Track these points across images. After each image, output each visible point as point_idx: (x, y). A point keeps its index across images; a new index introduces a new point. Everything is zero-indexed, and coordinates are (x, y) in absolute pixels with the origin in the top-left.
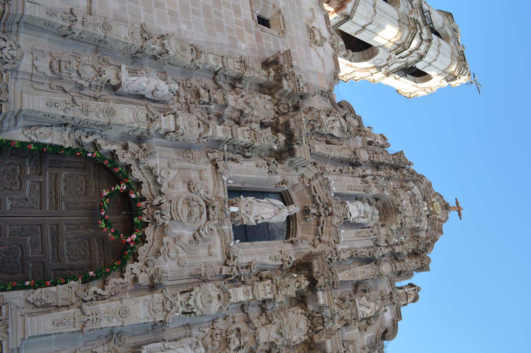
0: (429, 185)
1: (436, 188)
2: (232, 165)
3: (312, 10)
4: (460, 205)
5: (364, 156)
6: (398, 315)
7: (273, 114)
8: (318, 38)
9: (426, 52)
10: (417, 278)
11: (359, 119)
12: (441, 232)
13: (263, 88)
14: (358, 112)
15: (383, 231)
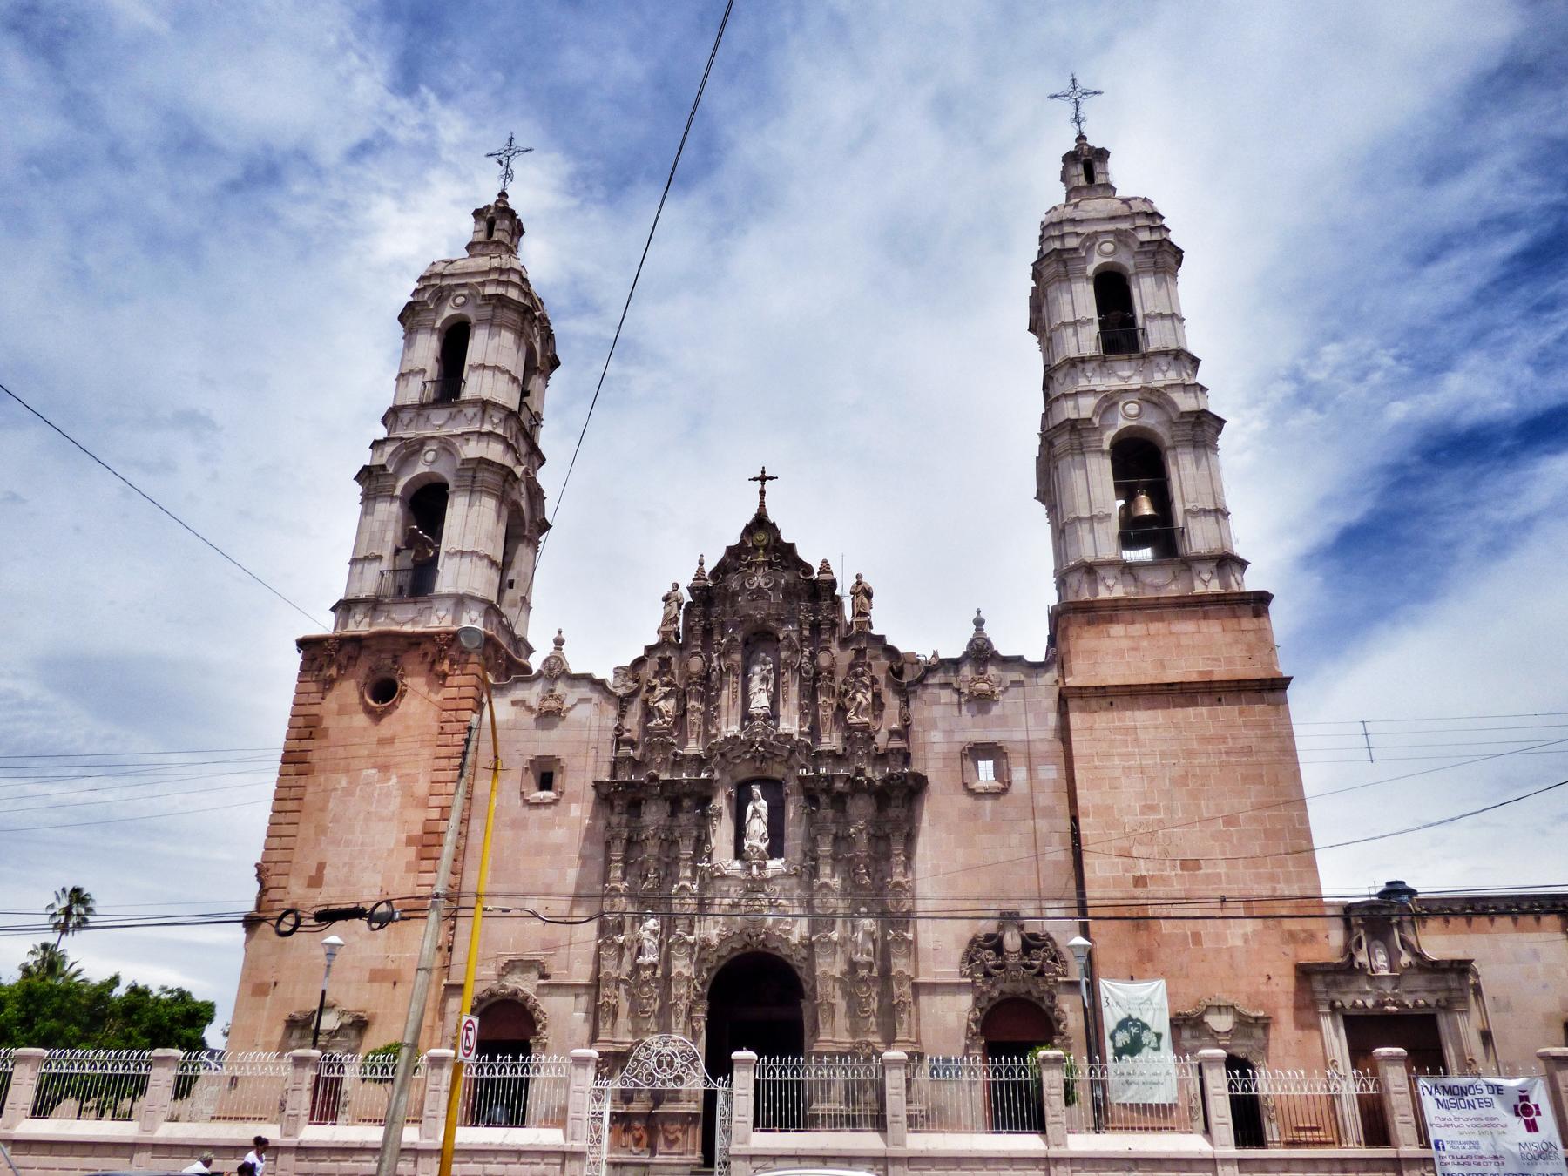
0: (729, 549)
1: (735, 540)
2: (716, 859)
3: (514, 703)
4: (759, 475)
5: (696, 664)
6: (881, 638)
7: (660, 802)
8: (553, 704)
9: (504, 407)
10: (844, 589)
11: (650, 650)
12: (791, 547)
13: (634, 807)
14: (641, 653)
15: (783, 655)
